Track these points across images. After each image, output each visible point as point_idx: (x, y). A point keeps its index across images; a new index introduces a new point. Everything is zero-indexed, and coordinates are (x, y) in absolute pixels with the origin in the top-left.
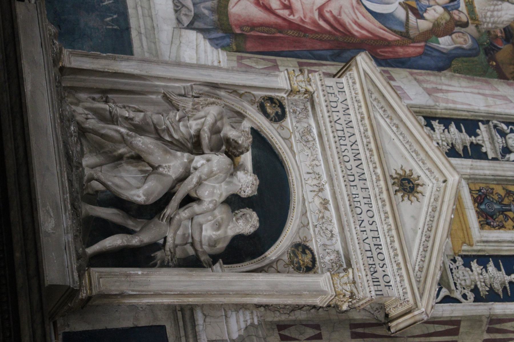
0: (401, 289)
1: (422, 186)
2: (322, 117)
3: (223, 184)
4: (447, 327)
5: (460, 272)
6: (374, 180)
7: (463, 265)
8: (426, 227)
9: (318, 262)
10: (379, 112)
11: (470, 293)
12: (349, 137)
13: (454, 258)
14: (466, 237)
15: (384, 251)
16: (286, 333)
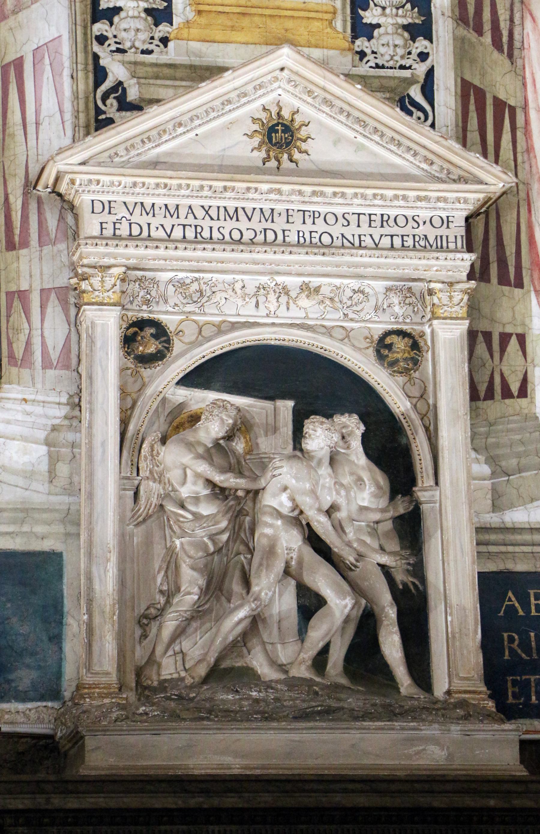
0: (458, 205)
1: (281, 109)
2: (166, 260)
3: (320, 472)
4: (472, 107)
5: (382, 50)
6: (277, 197)
7: (369, 40)
8: (357, 127)
9: (404, 327)
10: (149, 149)
11: (417, 44)
12: (196, 218)
13: (357, 52)
14: (320, 15)
15: (393, 213)
16: (482, 389)
